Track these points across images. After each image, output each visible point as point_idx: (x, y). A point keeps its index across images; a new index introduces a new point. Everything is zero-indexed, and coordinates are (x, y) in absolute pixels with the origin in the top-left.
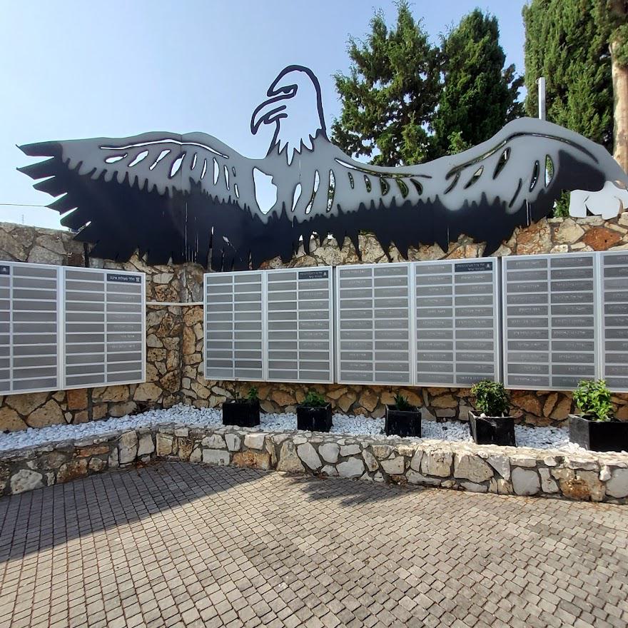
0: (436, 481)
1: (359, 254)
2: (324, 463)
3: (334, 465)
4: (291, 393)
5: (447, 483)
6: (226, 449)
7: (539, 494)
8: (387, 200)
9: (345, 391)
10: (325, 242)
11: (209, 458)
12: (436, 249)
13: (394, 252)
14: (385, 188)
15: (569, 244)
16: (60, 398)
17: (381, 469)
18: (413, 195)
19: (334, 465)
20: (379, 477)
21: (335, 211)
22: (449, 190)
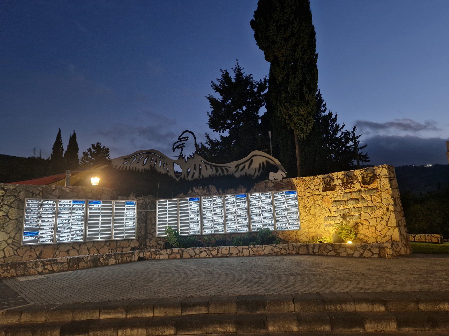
0: (225, 255)
1: (209, 191)
2: (196, 254)
3: (199, 254)
5: (228, 255)
6: (167, 254)
7: (250, 256)
8: (218, 174)
10: (198, 187)
11: (161, 257)
12: (233, 189)
13: (221, 191)
14: (217, 171)
15: (270, 188)
16: (108, 245)
17: (211, 254)
18: (226, 173)
19: (199, 254)
20: (211, 256)
21: (201, 177)
22: (236, 171)
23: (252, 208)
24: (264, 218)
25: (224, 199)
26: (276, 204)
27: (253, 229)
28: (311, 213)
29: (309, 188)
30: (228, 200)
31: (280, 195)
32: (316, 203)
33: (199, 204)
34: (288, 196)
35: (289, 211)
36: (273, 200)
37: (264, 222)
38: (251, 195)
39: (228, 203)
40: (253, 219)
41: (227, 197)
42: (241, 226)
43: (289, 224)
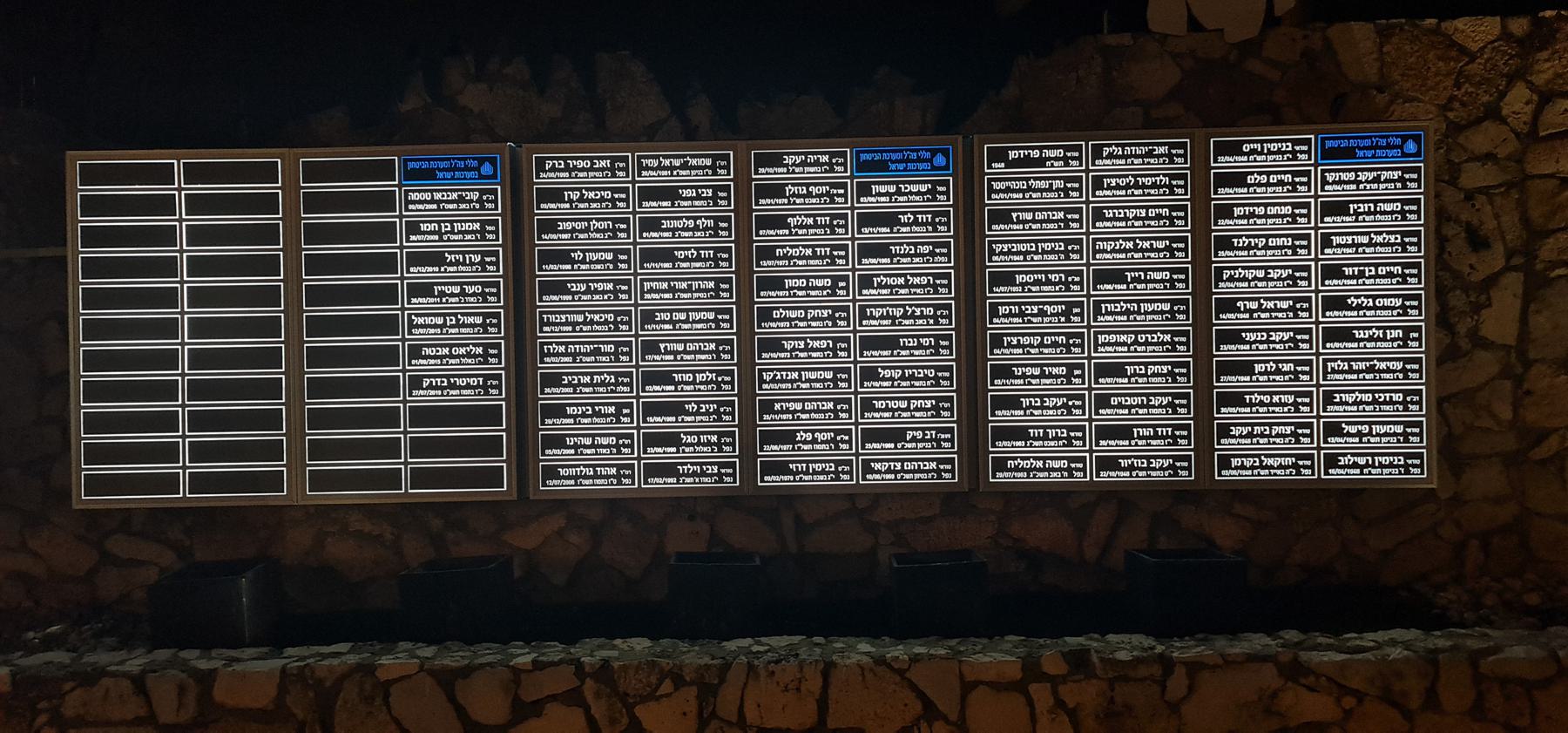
4: (388, 536)
9: (557, 521)
13: (700, 113)
23: (1007, 279)
24: (1104, 370)
25: (742, 179)
26: (1225, 243)
27: (1000, 465)
28: (1489, 330)
29: (1493, 113)
30: (776, 191)
31: (1271, 174)
32: (1548, 249)
33: (496, 211)
34: (1340, 183)
35: (1336, 317)
36: (1204, 213)
37: (1103, 401)
38: (998, 155)
39: (779, 222)
40: (1004, 372)
41: (777, 161)
42: (897, 436)
43: (1333, 429)
